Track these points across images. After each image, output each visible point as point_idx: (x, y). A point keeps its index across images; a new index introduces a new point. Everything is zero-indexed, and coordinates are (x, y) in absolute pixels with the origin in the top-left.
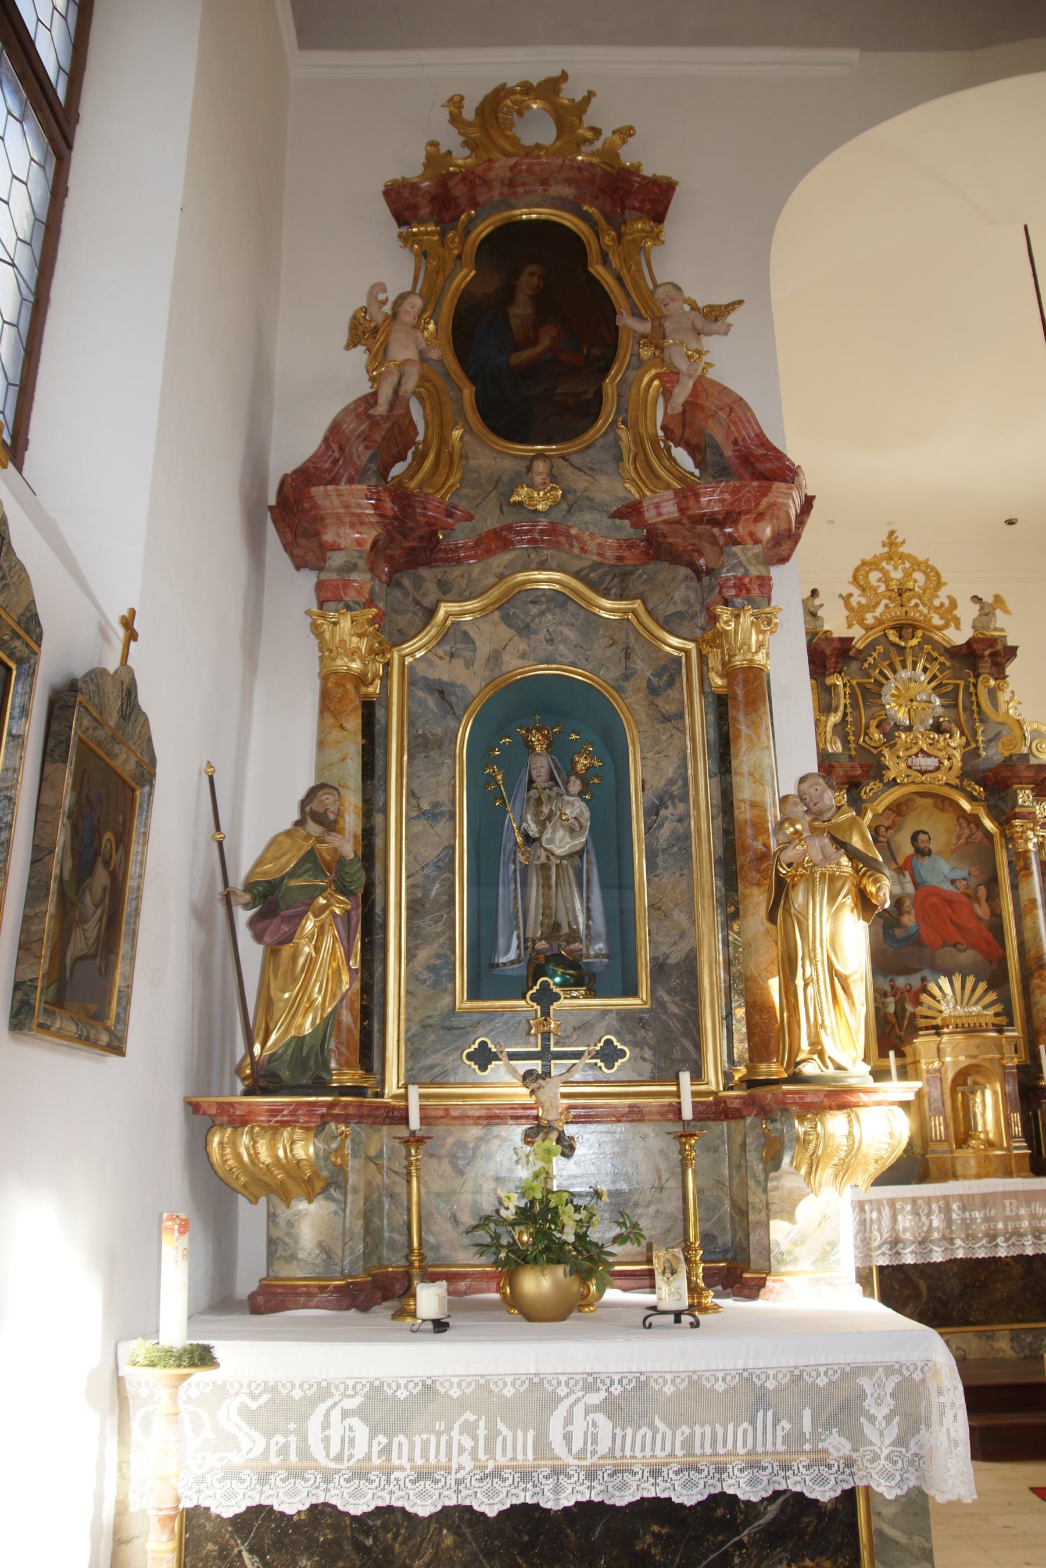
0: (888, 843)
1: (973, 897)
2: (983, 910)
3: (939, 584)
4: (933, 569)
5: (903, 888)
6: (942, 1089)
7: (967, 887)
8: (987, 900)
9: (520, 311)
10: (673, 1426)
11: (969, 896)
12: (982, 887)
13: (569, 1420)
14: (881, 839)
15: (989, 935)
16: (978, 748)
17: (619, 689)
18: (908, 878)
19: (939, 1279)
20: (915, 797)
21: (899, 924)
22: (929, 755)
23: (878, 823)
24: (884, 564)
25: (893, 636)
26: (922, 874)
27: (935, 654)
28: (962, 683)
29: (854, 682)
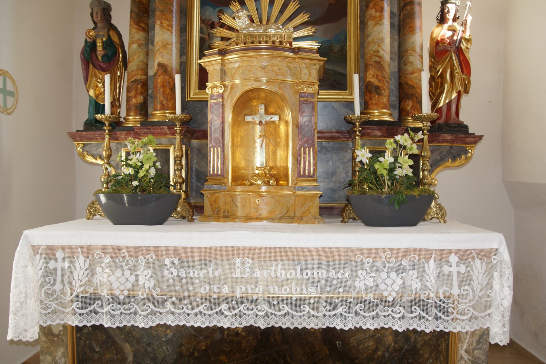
6: (223, 117)
19: (148, 345)
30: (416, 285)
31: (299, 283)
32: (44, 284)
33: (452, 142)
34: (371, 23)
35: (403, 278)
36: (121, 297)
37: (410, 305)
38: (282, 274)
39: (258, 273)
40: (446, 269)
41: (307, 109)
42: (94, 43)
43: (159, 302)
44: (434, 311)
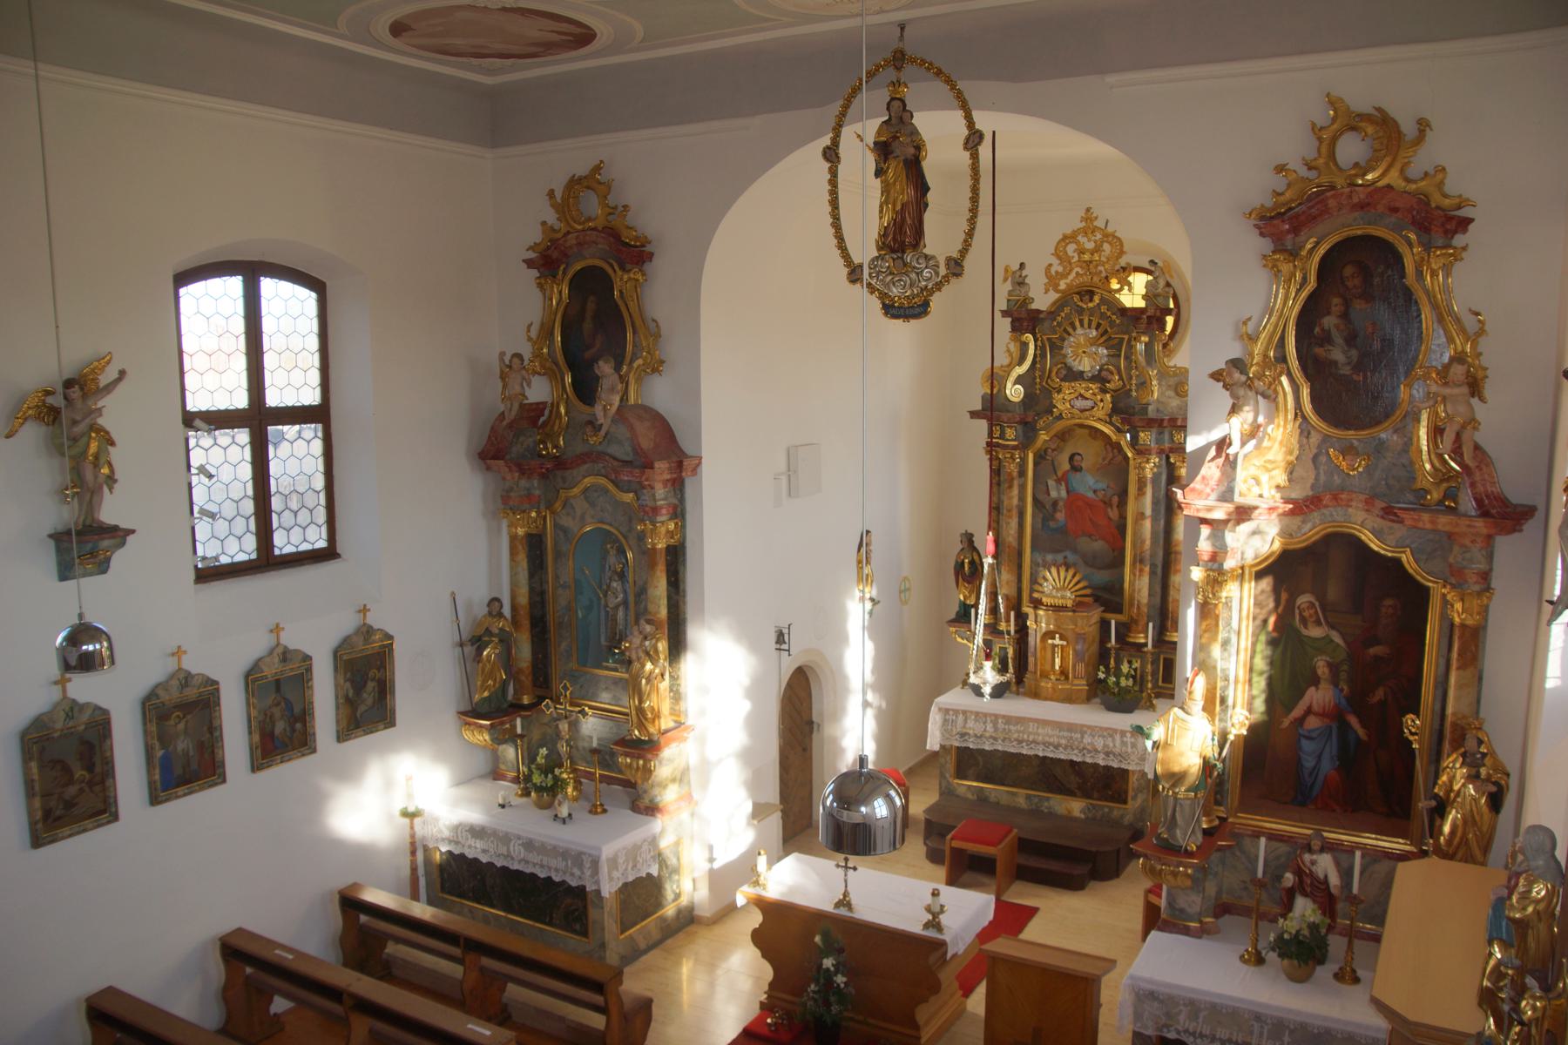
0: (1053, 461)
1: (1108, 503)
2: (1113, 514)
3: (1122, 253)
4: (1119, 239)
5: (1059, 493)
7: (1105, 495)
9: (588, 325)
11: (1105, 503)
16: (1131, 390)
17: (625, 537)
18: (1063, 487)
20: (1076, 428)
21: (1053, 518)
22: (1087, 399)
23: (1047, 446)
24: (1079, 238)
25: (1076, 298)
27: (1109, 313)
28: (1126, 337)
29: (1045, 337)
30: (1111, 745)
31: (1058, 737)
32: (943, 725)
37: (1107, 754)
38: (1050, 732)
39: (1040, 731)
40: (1125, 739)
42: (963, 562)
43: (995, 739)
44: (1120, 758)
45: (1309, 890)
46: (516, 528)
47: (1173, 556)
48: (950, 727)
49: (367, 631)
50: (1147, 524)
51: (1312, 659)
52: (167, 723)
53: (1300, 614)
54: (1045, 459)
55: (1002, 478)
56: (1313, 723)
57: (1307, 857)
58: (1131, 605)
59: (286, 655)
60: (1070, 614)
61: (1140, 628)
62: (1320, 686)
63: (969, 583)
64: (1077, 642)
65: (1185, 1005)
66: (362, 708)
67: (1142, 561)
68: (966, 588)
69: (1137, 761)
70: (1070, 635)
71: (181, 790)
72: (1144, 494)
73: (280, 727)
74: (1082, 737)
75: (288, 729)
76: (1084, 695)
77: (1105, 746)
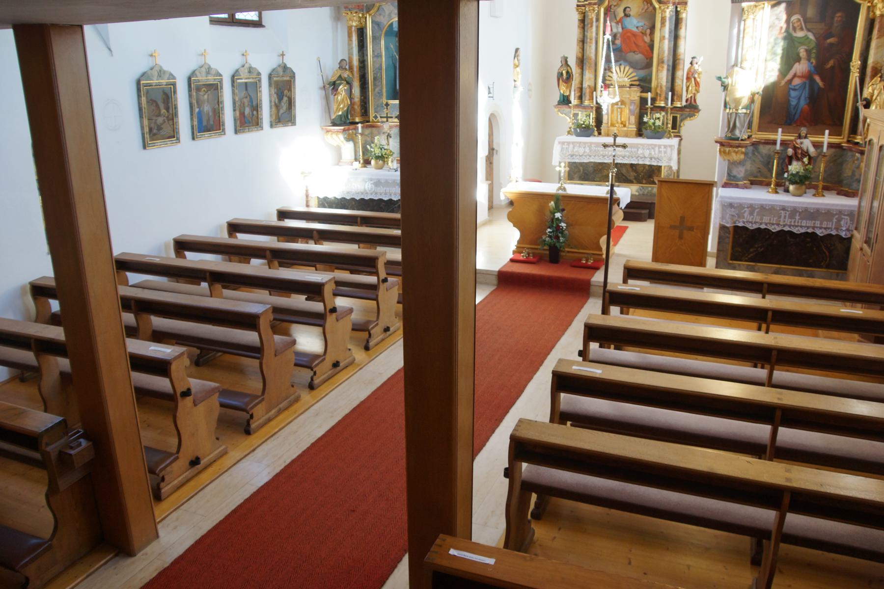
0: (614, 12)
1: (644, 34)
2: (647, 39)
7: (642, 29)
8: (649, 35)
10: (383, 187)
11: (643, 33)
12: (649, 30)
13: (368, 185)
14: (612, 10)
15: (648, 48)
26: (626, 24)
30: (653, 153)
32: (561, 151)
33: (689, 111)
34: (659, 72)
35: (650, 151)
36: (581, 155)
40: (660, 149)
41: (633, 104)
44: (658, 160)
45: (800, 156)
46: (352, 22)
47: (678, 61)
48: (565, 152)
49: (285, 68)
50: (666, 42)
51: (798, 49)
52: (200, 93)
53: (793, 26)
54: (610, 11)
55: (586, 23)
56: (797, 82)
57: (799, 141)
58: (656, 89)
59: (251, 70)
60: (628, 89)
61: (662, 98)
62: (802, 62)
63: (566, 83)
64: (631, 105)
65: (748, 208)
66: (281, 111)
67: (663, 62)
68: (564, 86)
69: (667, 160)
70: (627, 101)
71: (207, 134)
72: (665, 26)
73: (247, 111)
74: (638, 150)
75: (251, 113)
76: (634, 133)
77: (650, 154)
